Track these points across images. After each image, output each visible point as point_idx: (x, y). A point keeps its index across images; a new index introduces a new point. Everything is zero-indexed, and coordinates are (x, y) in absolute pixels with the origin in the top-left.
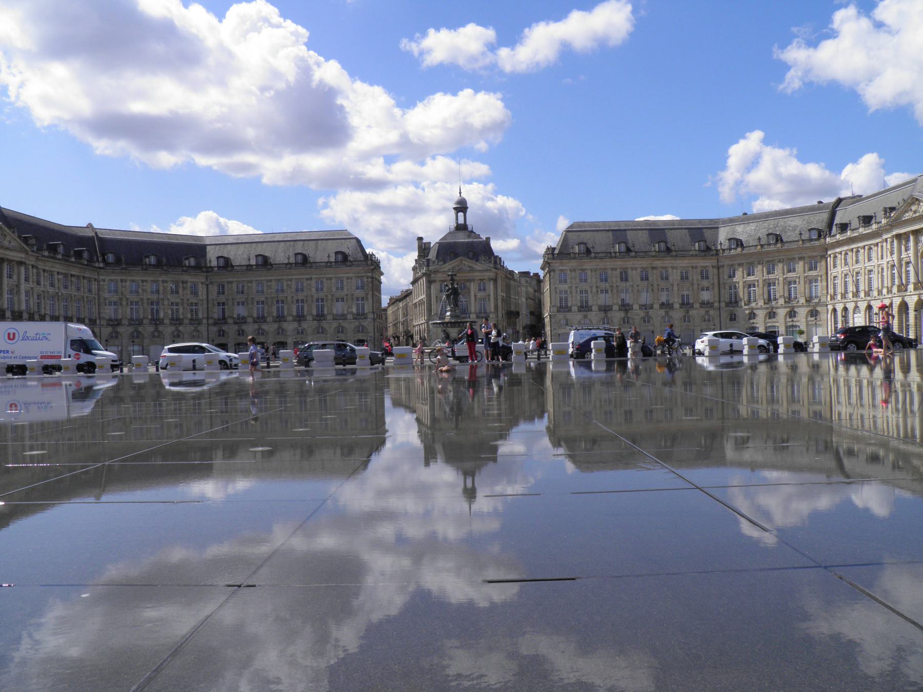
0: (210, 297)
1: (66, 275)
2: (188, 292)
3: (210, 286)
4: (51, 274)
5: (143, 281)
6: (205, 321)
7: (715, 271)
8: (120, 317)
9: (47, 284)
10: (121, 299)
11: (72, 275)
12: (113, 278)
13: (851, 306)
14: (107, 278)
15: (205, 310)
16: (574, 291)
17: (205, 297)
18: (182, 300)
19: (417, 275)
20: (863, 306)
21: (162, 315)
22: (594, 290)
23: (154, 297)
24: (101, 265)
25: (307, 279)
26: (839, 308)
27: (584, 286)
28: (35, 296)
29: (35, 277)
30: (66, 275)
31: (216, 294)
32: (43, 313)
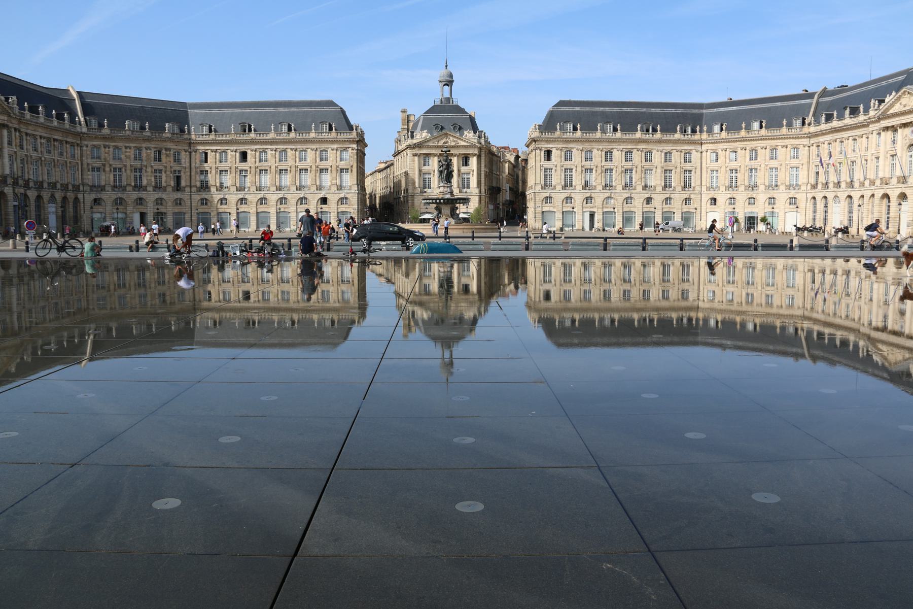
0: (193, 165)
1: (48, 140)
2: (172, 160)
3: (193, 154)
4: (34, 136)
5: (126, 147)
6: (188, 189)
7: (699, 154)
8: (103, 183)
9: (30, 148)
10: (104, 165)
11: (55, 140)
12: (95, 143)
13: (830, 196)
14: (90, 143)
15: (188, 177)
16: (559, 168)
17: (188, 164)
18: (166, 167)
19: (400, 148)
20: (843, 195)
21: (145, 182)
22: (579, 169)
23: (137, 164)
24: (84, 130)
25: (292, 149)
26: (819, 196)
27: (568, 164)
28: (19, 161)
29: (18, 141)
30: (48, 140)
31: (198, 163)
32: (26, 178)
